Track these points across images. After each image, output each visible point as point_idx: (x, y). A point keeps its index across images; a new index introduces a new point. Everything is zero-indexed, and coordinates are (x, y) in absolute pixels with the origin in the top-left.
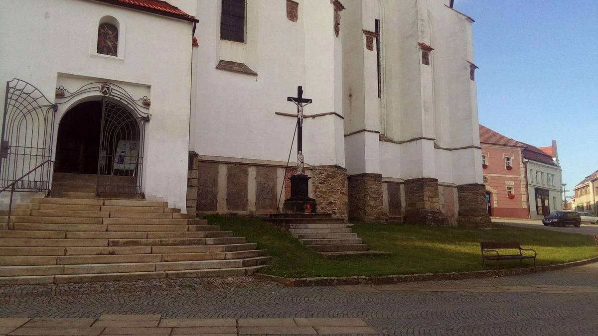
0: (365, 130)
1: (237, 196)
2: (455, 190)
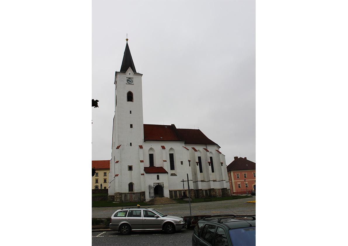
0: (198, 181)
1: (176, 196)
2: (221, 190)
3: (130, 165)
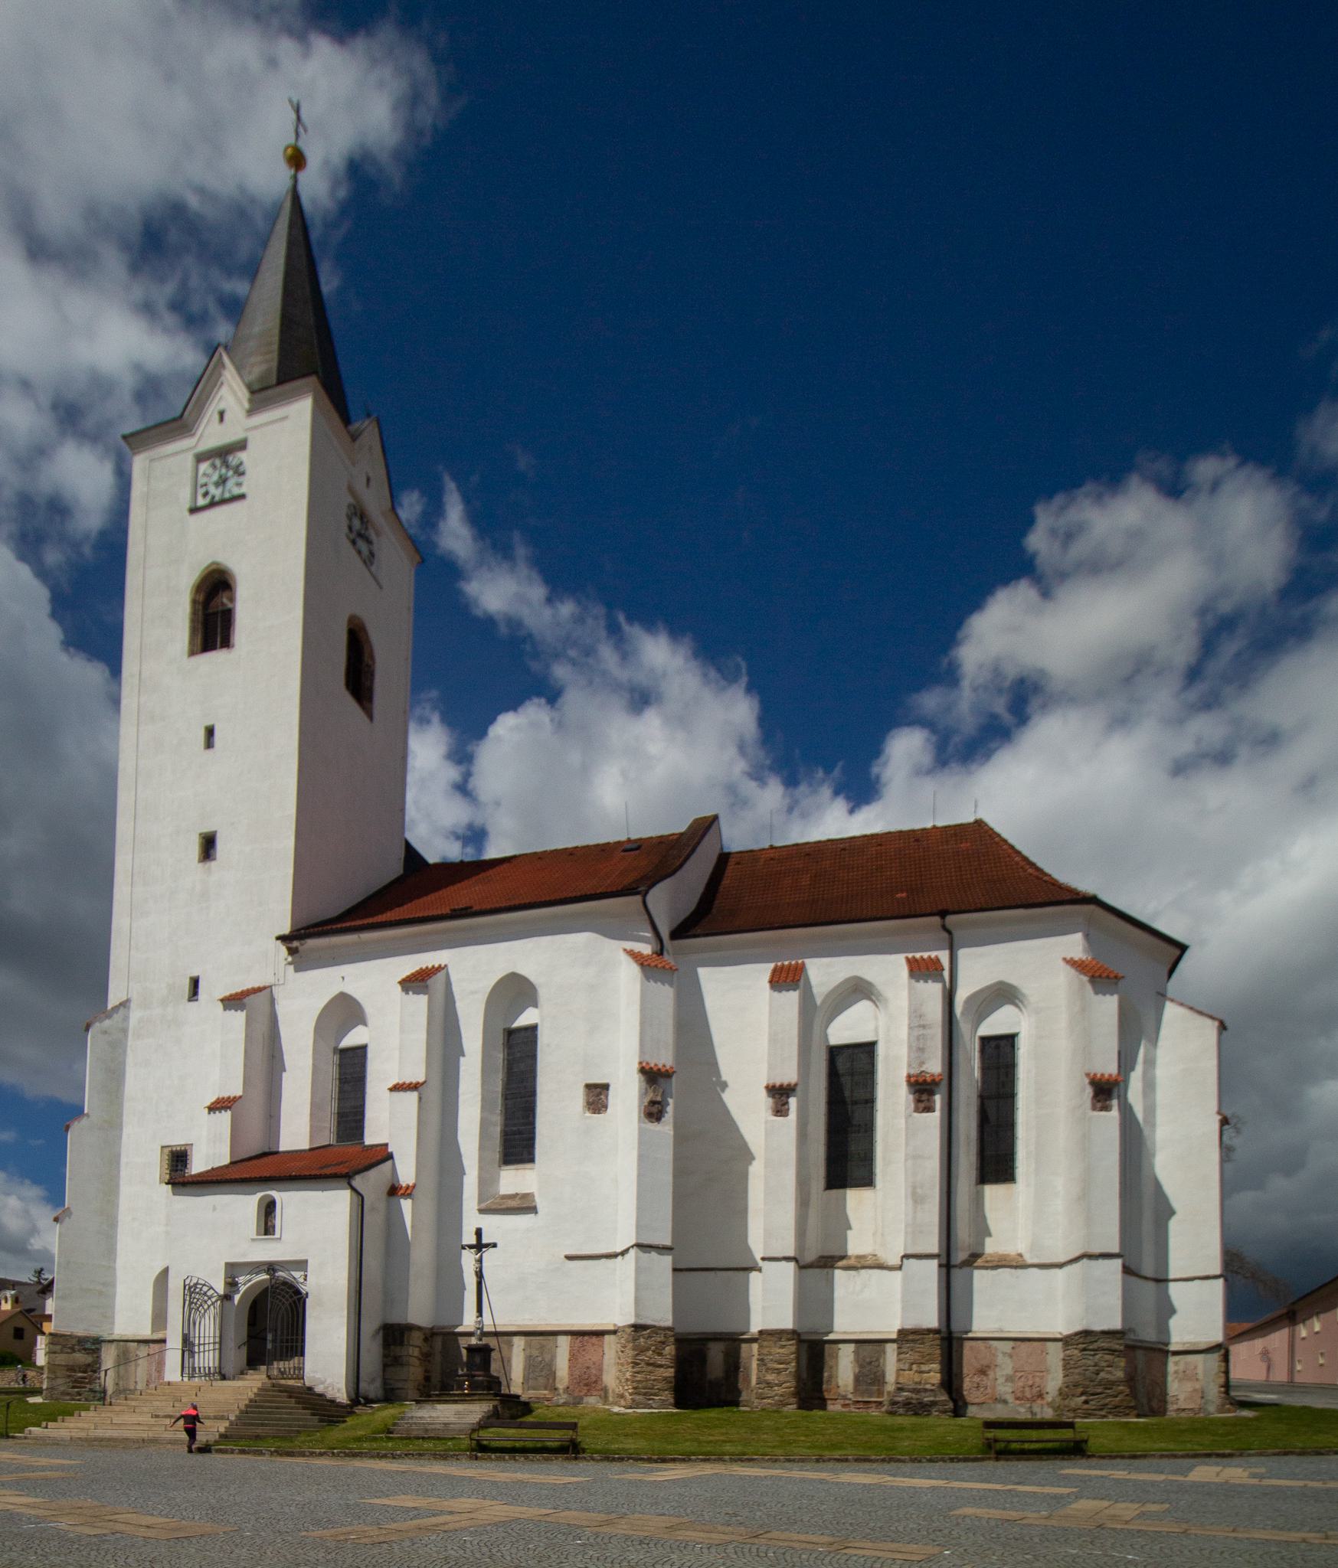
3: (177, 1141)
